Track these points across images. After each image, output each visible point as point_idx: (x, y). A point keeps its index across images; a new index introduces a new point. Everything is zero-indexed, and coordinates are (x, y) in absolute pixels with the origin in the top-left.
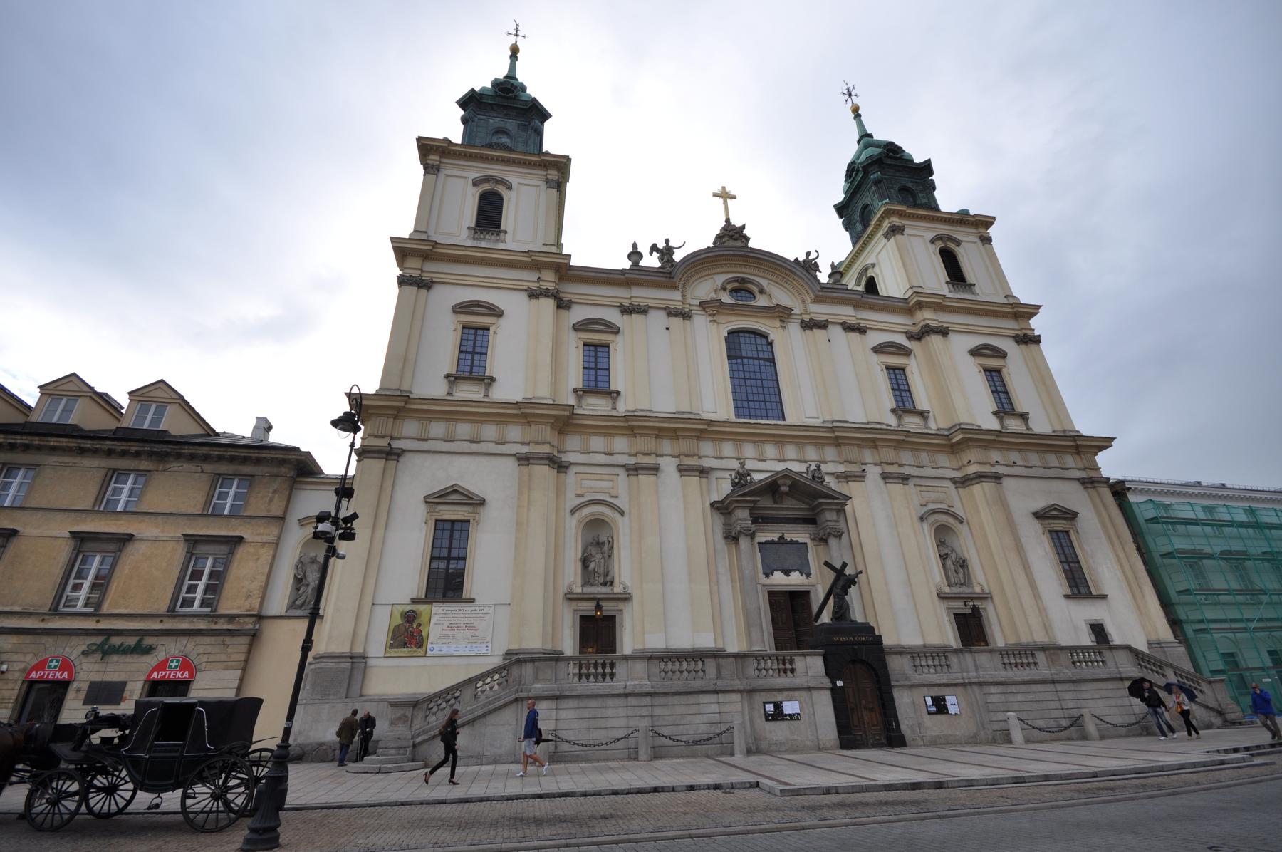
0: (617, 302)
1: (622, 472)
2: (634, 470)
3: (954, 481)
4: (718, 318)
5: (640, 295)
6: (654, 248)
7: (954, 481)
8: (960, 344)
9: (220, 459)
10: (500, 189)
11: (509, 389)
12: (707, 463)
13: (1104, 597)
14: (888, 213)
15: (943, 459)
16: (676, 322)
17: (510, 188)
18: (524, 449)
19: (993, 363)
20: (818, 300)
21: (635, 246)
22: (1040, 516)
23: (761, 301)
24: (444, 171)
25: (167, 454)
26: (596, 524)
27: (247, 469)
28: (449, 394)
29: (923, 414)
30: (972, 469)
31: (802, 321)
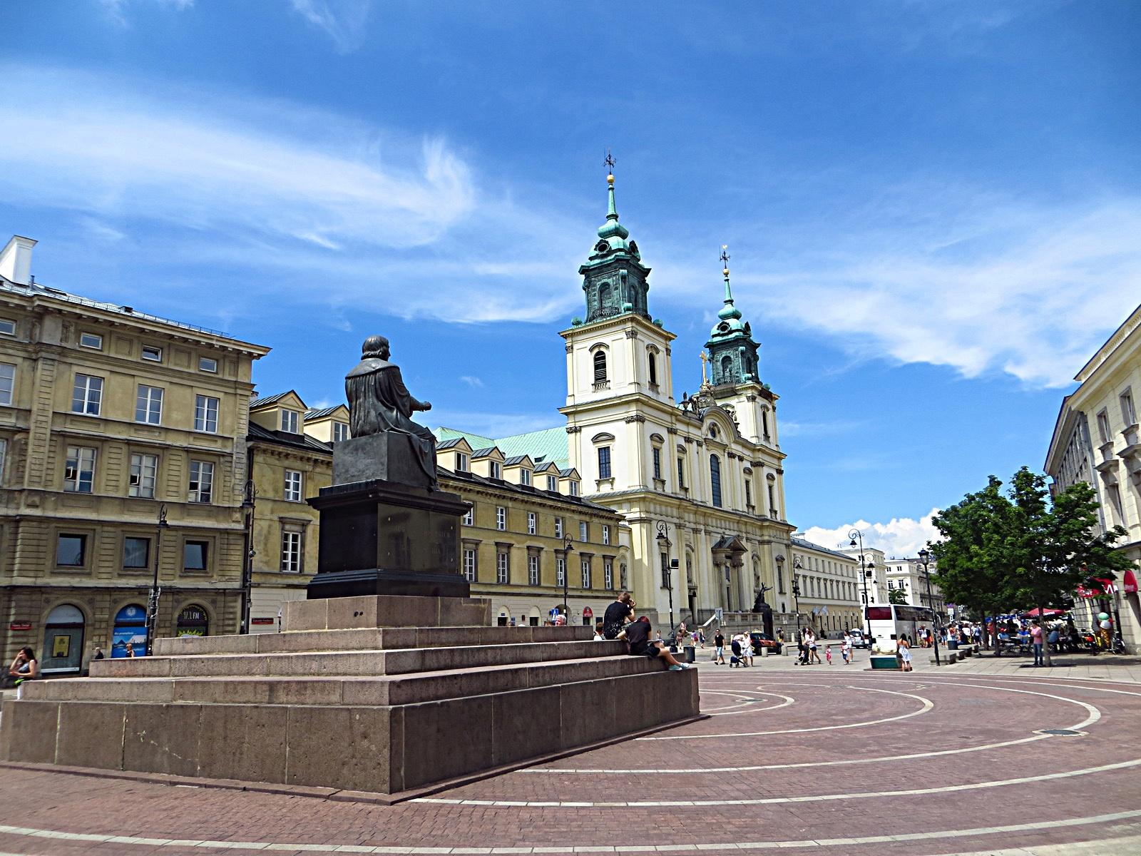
0: (686, 435)
1: (691, 530)
2: (696, 531)
3: (759, 541)
4: (710, 448)
5: (694, 433)
6: (691, 400)
7: (759, 541)
8: (766, 471)
9: (602, 517)
10: (654, 353)
11: (668, 490)
12: (711, 529)
13: (785, 593)
14: (753, 388)
15: (758, 532)
16: (700, 448)
17: (658, 351)
18: (677, 521)
19: (771, 483)
20: (735, 442)
21: (685, 396)
22: (777, 560)
23: (717, 440)
24: (638, 336)
25: (595, 515)
26: (688, 555)
27: (610, 523)
28: (655, 489)
29: (753, 507)
30: (766, 538)
31: (728, 453)
